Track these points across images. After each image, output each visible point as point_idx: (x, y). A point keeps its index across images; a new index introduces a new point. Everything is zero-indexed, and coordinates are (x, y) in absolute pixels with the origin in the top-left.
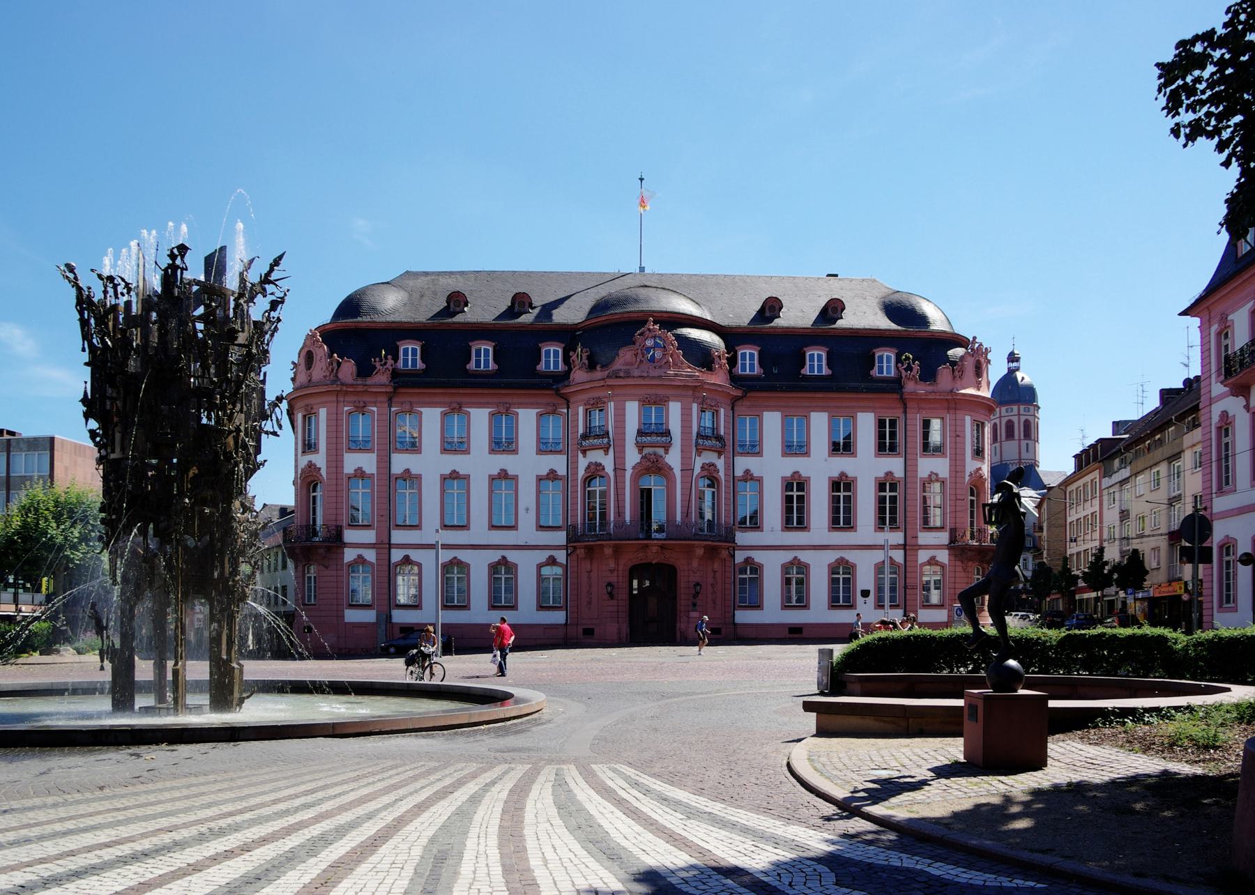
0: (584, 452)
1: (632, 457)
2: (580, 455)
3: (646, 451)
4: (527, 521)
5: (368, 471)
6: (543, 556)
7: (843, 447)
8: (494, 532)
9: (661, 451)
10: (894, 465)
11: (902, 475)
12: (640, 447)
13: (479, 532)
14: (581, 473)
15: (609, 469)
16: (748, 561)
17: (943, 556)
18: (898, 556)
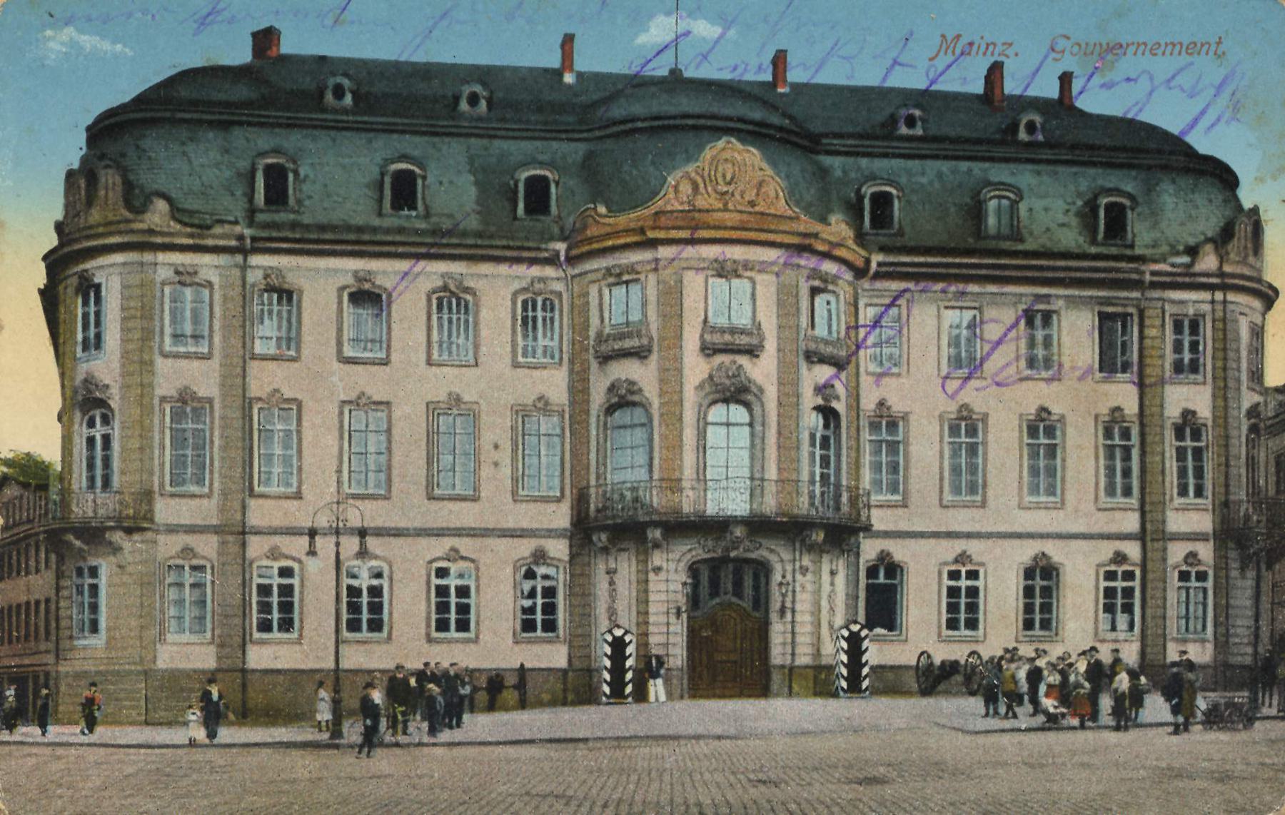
0: (605, 359)
1: (696, 369)
2: (594, 365)
3: (720, 359)
4: (495, 481)
5: (202, 393)
6: (525, 548)
7: (1041, 361)
8: (435, 505)
9: (743, 360)
10: (1124, 395)
11: (1135, 410)
12: (709, 350)
13: (407, 506)
14: (598, 397)
15: (651, 391)
16: (884, 557)
17: (1206, 552)
18: (1133, 550)
